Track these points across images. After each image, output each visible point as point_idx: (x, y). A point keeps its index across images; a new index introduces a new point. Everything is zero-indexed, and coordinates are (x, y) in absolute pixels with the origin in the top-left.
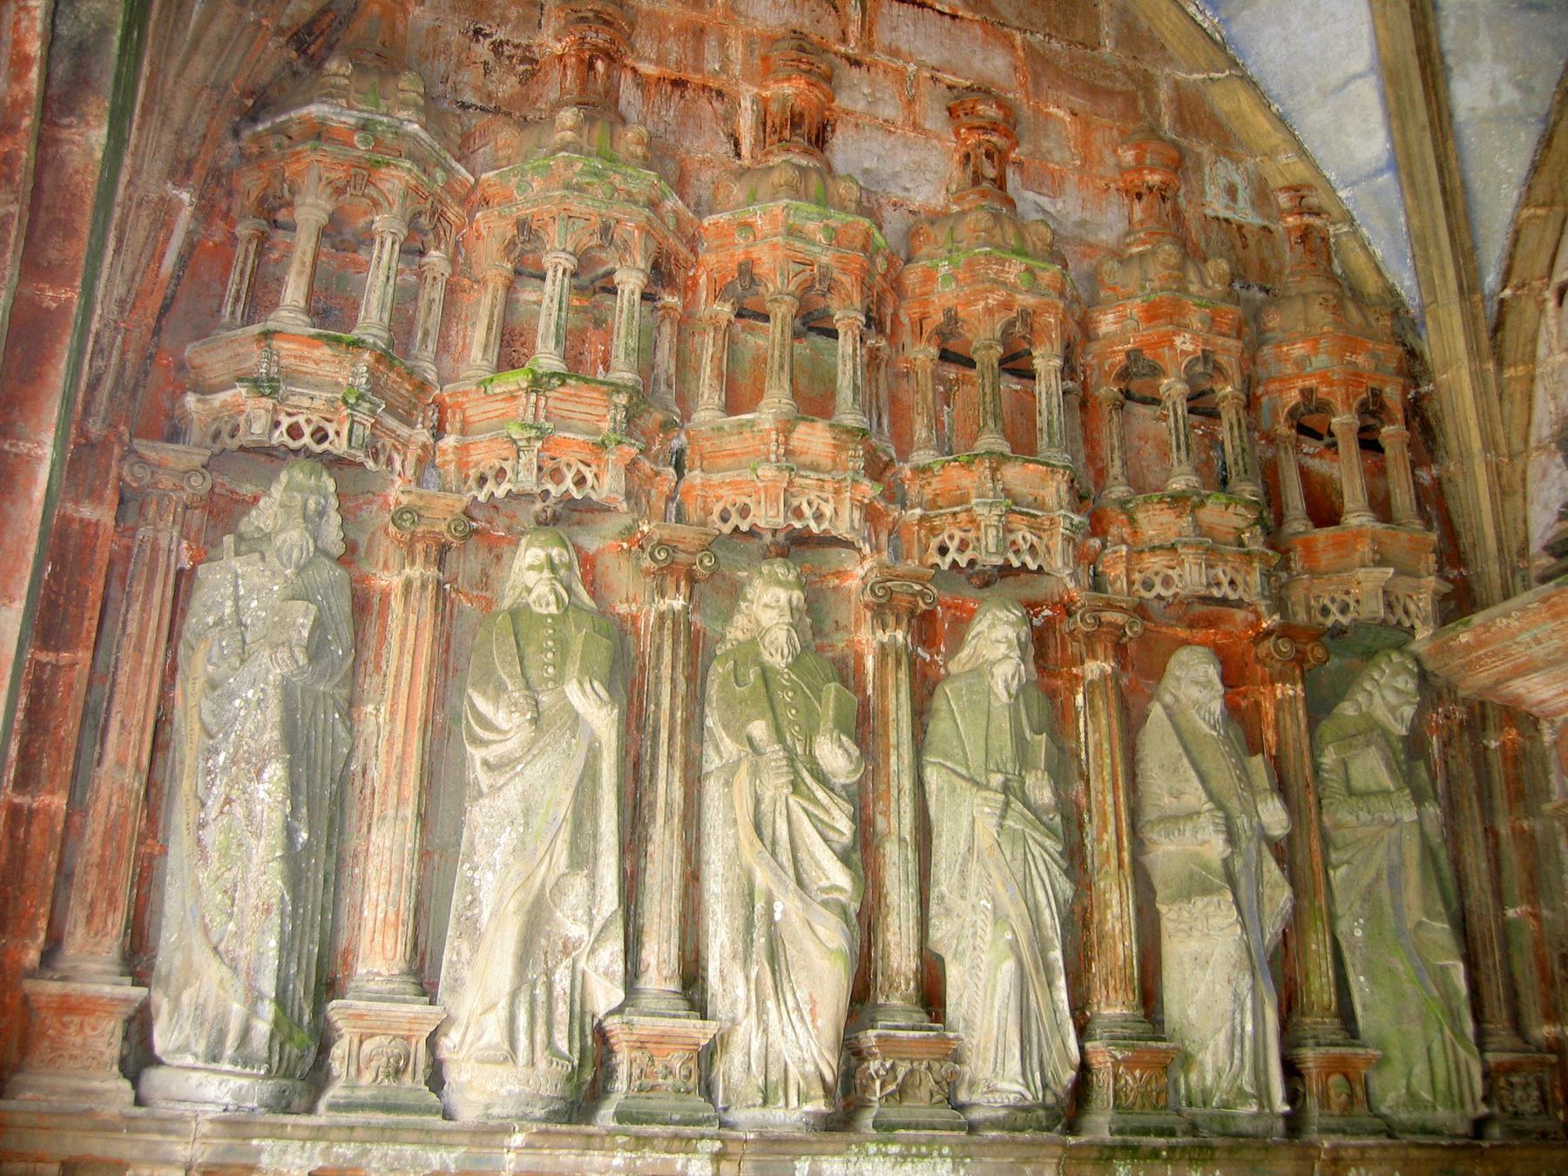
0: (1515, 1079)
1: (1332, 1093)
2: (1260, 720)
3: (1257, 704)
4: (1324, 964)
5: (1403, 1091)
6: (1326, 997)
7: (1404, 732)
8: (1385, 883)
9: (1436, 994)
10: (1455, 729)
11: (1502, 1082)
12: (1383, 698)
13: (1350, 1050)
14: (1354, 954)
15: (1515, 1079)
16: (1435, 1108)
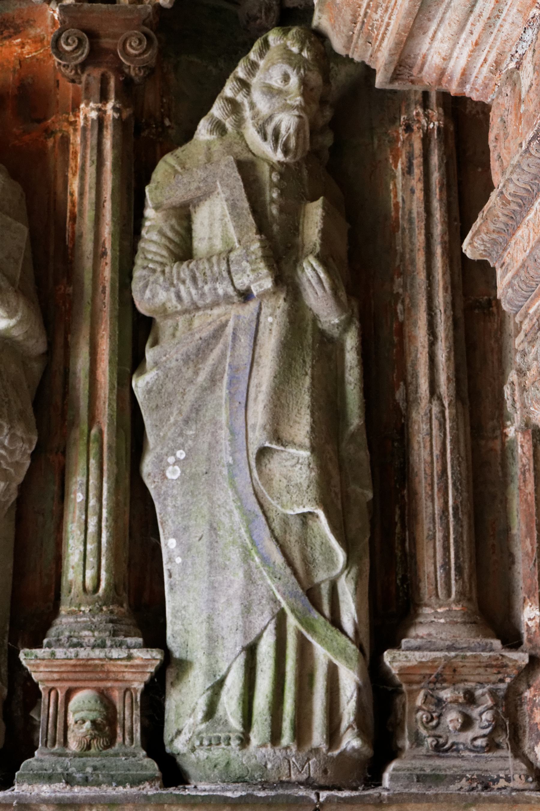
0: (446, 694)
1: (71, 719)
2: (66, 164)
3: (65, 141)
4: (92, 522)
5: (200, 715)
6: (90, 573)
7: (279, 156)
8: (223, 391)
9: (278, 558)
10: (417, 146)
11: (419, 702)
12: (252, 106)
13: (98, 653)
14: (165, 506)
15: (446, 694)
16: (244, 741)
